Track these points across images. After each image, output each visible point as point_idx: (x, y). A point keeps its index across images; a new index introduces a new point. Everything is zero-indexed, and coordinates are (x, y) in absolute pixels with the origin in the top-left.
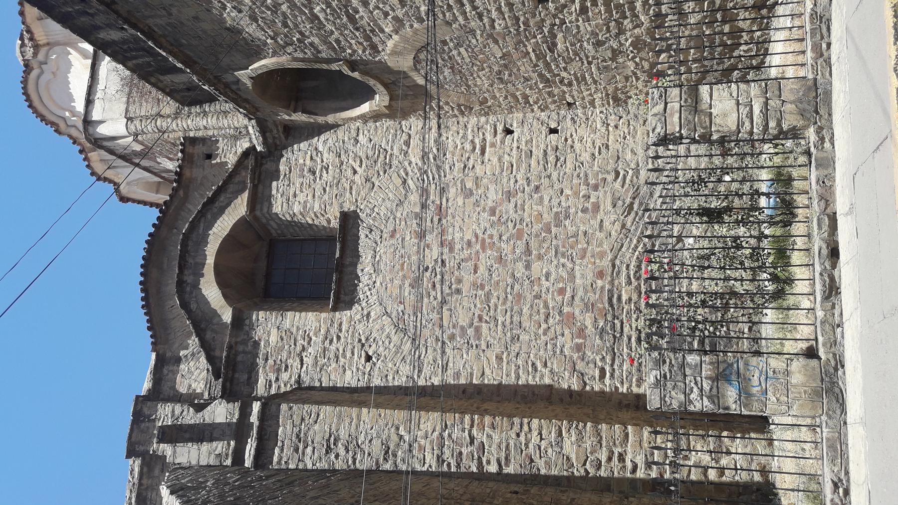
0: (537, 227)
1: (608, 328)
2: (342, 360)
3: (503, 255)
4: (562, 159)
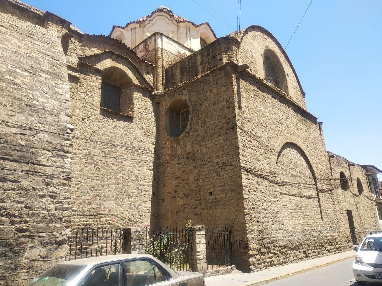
0: (126, 187)
1: (91, 213)
2: (82, 109)
4: (146, 197)
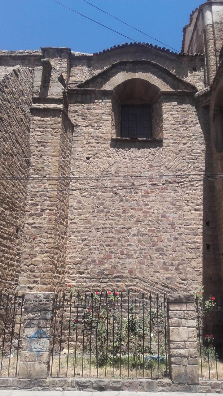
0: (155, 239)
1: (104, 276)
2: (86, 146)
3: (141, 222)
4: (193, 251)
